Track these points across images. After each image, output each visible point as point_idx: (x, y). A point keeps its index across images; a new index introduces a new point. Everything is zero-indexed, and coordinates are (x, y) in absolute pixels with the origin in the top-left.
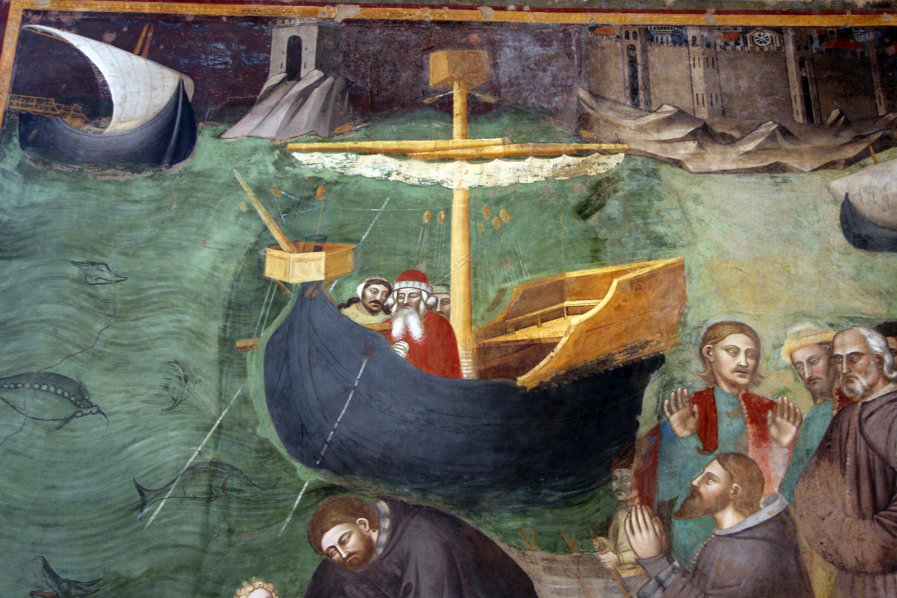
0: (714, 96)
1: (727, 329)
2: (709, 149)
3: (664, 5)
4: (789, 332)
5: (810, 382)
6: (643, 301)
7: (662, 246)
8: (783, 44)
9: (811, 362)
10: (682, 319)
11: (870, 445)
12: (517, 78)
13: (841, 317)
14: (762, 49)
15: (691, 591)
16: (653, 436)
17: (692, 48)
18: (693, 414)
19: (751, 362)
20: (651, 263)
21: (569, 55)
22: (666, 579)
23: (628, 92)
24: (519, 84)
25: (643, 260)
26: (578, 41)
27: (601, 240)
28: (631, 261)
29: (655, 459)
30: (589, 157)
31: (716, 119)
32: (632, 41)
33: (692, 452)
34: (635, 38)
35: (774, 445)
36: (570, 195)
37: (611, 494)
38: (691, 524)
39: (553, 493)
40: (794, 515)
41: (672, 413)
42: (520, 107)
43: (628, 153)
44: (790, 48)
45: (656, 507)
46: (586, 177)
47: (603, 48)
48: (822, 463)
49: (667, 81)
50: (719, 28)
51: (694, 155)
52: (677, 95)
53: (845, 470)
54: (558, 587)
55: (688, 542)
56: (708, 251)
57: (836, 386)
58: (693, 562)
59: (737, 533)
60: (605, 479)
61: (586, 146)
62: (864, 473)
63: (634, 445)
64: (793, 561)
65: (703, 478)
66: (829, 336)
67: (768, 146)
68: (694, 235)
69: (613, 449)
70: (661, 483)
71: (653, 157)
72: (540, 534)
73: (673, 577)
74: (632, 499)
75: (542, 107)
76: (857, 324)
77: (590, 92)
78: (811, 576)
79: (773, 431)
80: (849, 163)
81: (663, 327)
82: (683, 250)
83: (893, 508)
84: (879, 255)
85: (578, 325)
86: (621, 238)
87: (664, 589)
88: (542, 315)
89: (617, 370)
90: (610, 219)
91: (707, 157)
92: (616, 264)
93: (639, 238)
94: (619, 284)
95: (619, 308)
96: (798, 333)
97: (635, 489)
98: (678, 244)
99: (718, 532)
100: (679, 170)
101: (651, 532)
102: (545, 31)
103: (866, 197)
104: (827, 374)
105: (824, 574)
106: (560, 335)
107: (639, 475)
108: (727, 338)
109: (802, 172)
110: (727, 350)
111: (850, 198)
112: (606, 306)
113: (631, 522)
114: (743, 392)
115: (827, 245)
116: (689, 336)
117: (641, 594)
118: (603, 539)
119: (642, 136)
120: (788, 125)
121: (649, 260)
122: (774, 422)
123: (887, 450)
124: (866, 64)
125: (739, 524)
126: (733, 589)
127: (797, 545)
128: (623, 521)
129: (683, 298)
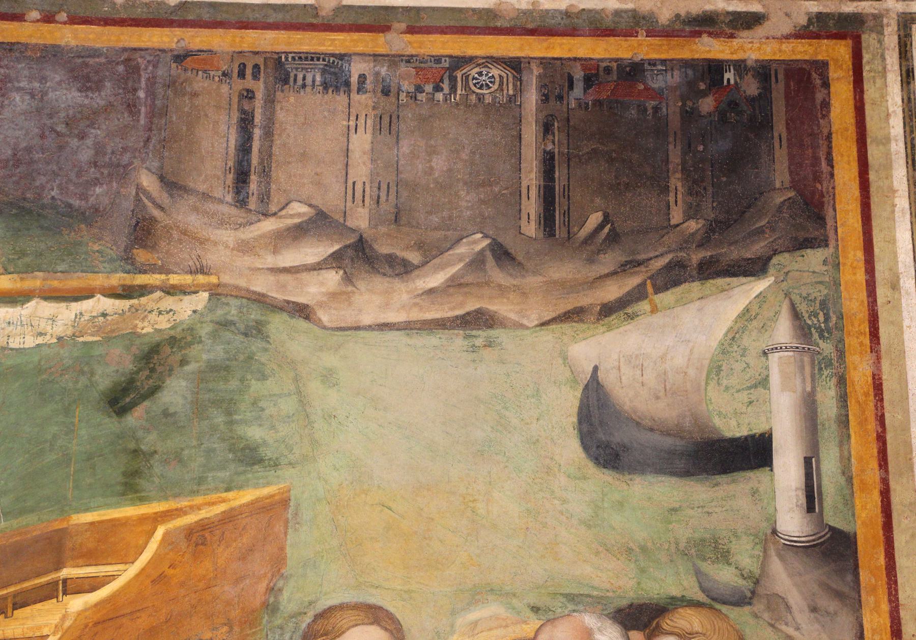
0: (384, 187)
1: (349, 617)
2: (362, 285)
3: (317, 15)
6: (205, 567)
7: (254, 464)
8: (520, 90)
10: (272, 600)
12: (29, 150)
14: (480, 98)
17: (355, 96)
20: (230, 495)
21: (132, 107)
23: (231, 177)
24: (31, 162)
25: (217, 489)
26: (152, 81)
27: (144, 453)
28: (194, 493)
30: (143, 300)
31: (383, 229)
32: (249, 82)
34: (256, 76)
36: (99, 370)
42: (27, 205)
43: (216, 293)
44: (531, 98)
46: (135, 334)
47: (195, 95)
49: (304, 157)
50: (409, 59)
51: (333, 296)
52: (319, 184)
56: (335, 474)
61: (141, 279)
67: (469, 278)
68: (314, 443)
71: (260, 300)
75: (70, 206)
76: (581, 607)
77: (162, 178)
80: (608, 310)
81: (235, 613)
82: (292, 471)
84: (638, 479)
85: (79, 614)
86: (182, 449)
88: (15, 595)
90: (166, 414)
91: (357, 299)
92: (166, 498)
93: (214, 450)
94: (166, 534)
95: (160, 579)
96: (475, 623)
98: (284, 461)
100: (302, 324)
102: (91, 61)
103: (628, 373)
106: (45, 631)
108: (348, 633)
109: (523, 326)
111: (601, 375)
112: (138, 576)
115: (548, 461)
116: (279, 631)
119: (247, 261)
120: (508, 240)
121: (228, 490)
124: (660, 129)
129: (279, 560)
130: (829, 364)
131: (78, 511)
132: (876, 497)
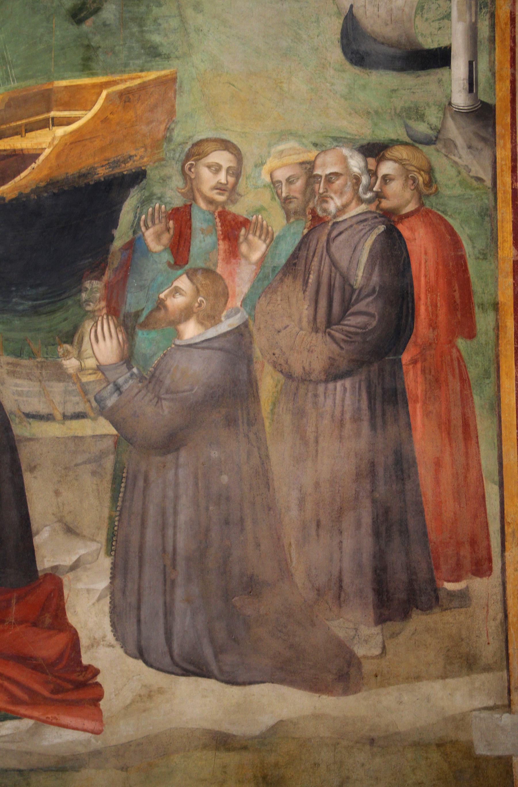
4: (273, 150)
5: (287, 201)
7: (156, 57)
9: (289, 181)
10: (168, 135)
11: (334, 263)
13: (326, 137)
15: (145, 395)
16: (126, 250)
18: (168, 229)
19: (231, 180)
20: (143, 74)
22: (124, 384)
25: (135, 70)
27: (93, 48)
28: (123, 72)
29: (126, 271)
33: (162, 266)
35: (243, 261)
37: (80, 304)
38: (153, 334)
39: (22, 302)
40: (253, 327)
41: (147, 228)
45: (122, 318)
48: (286, 280)
53: (307, 287)
54: (19, 389)
55: (148, 351)
56: (202, 64)
57: (311, 205)
58: (151, 369)
59: (196, 344)
60: (74, 290)
62: (324, 289)
63: (107, 258)
64: (244, 369)
65: (171, 292)
66: (310, 156)
68: (190, 46)
69: (86, 261)
70: (129, 295)
72: (7, 340)
73: (131, 382)
74: (100, 310)
76: (341, 144)
78: (259, 384)
79: (244, 248)
81: (148, 141)
82: (177, 61)
83: (346, 322)
85: (62, 137)
86: (115, 46)
87: (121, 393)
88: (26, 124)
89: (98, 184)
90: (105, 25)
92: (106, 74)
93: (133, 48)
94: (108, 95)
95: (106, 120)
96: (282, 152)
97: (103, 300)
98: (172, 56)
99: (178, 342)
101: (115, 341)
103: (370, 9)
104: (304, 193)
105: (272, 381)
106: (44, 146)
107: (109, 287)
108: (211, 155)
110: (209, 167)
111: (354, 10)
112: (93, 118)
113: (96, 331)
114: (220, 209)
115: (323, 61)
116: (172, 152)
117: (98, 397)
118: (68, 347)
121: (142, 71)
122: (246, 239)
123: (348, 269)
125: (199, 335)
126: (185, 394)
127: (251, 355)
128: (89, 330)
129: (171, 113)
130: (486, 6)
131: (58, 79)
132: (508, 84)
